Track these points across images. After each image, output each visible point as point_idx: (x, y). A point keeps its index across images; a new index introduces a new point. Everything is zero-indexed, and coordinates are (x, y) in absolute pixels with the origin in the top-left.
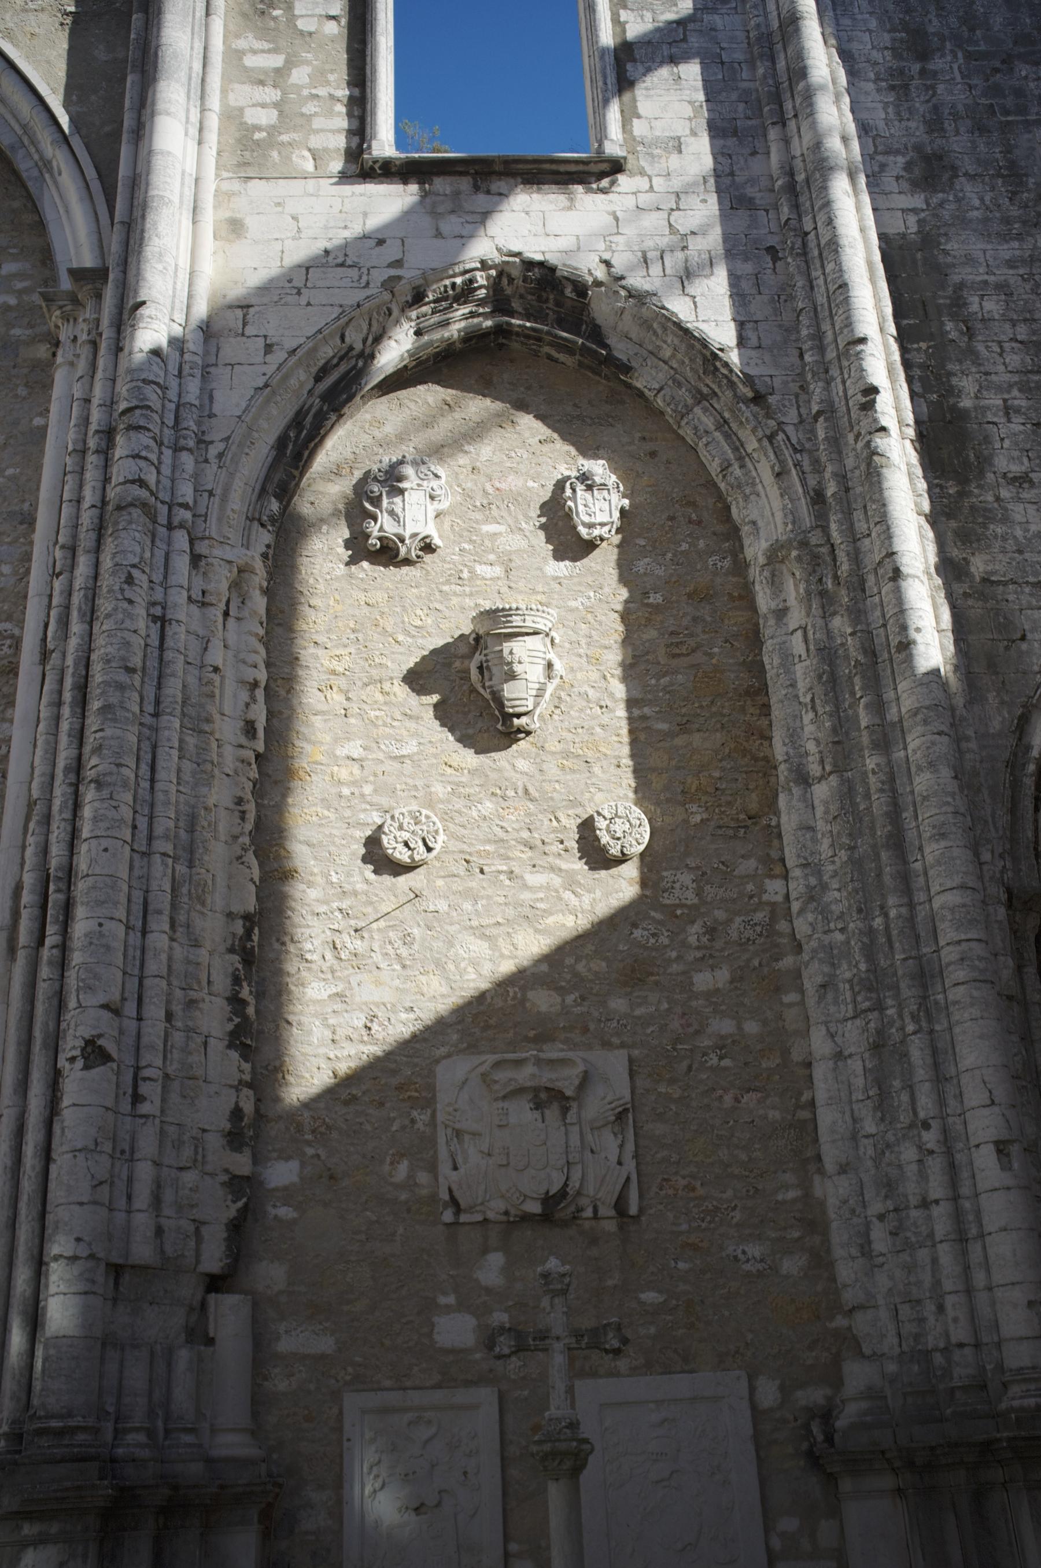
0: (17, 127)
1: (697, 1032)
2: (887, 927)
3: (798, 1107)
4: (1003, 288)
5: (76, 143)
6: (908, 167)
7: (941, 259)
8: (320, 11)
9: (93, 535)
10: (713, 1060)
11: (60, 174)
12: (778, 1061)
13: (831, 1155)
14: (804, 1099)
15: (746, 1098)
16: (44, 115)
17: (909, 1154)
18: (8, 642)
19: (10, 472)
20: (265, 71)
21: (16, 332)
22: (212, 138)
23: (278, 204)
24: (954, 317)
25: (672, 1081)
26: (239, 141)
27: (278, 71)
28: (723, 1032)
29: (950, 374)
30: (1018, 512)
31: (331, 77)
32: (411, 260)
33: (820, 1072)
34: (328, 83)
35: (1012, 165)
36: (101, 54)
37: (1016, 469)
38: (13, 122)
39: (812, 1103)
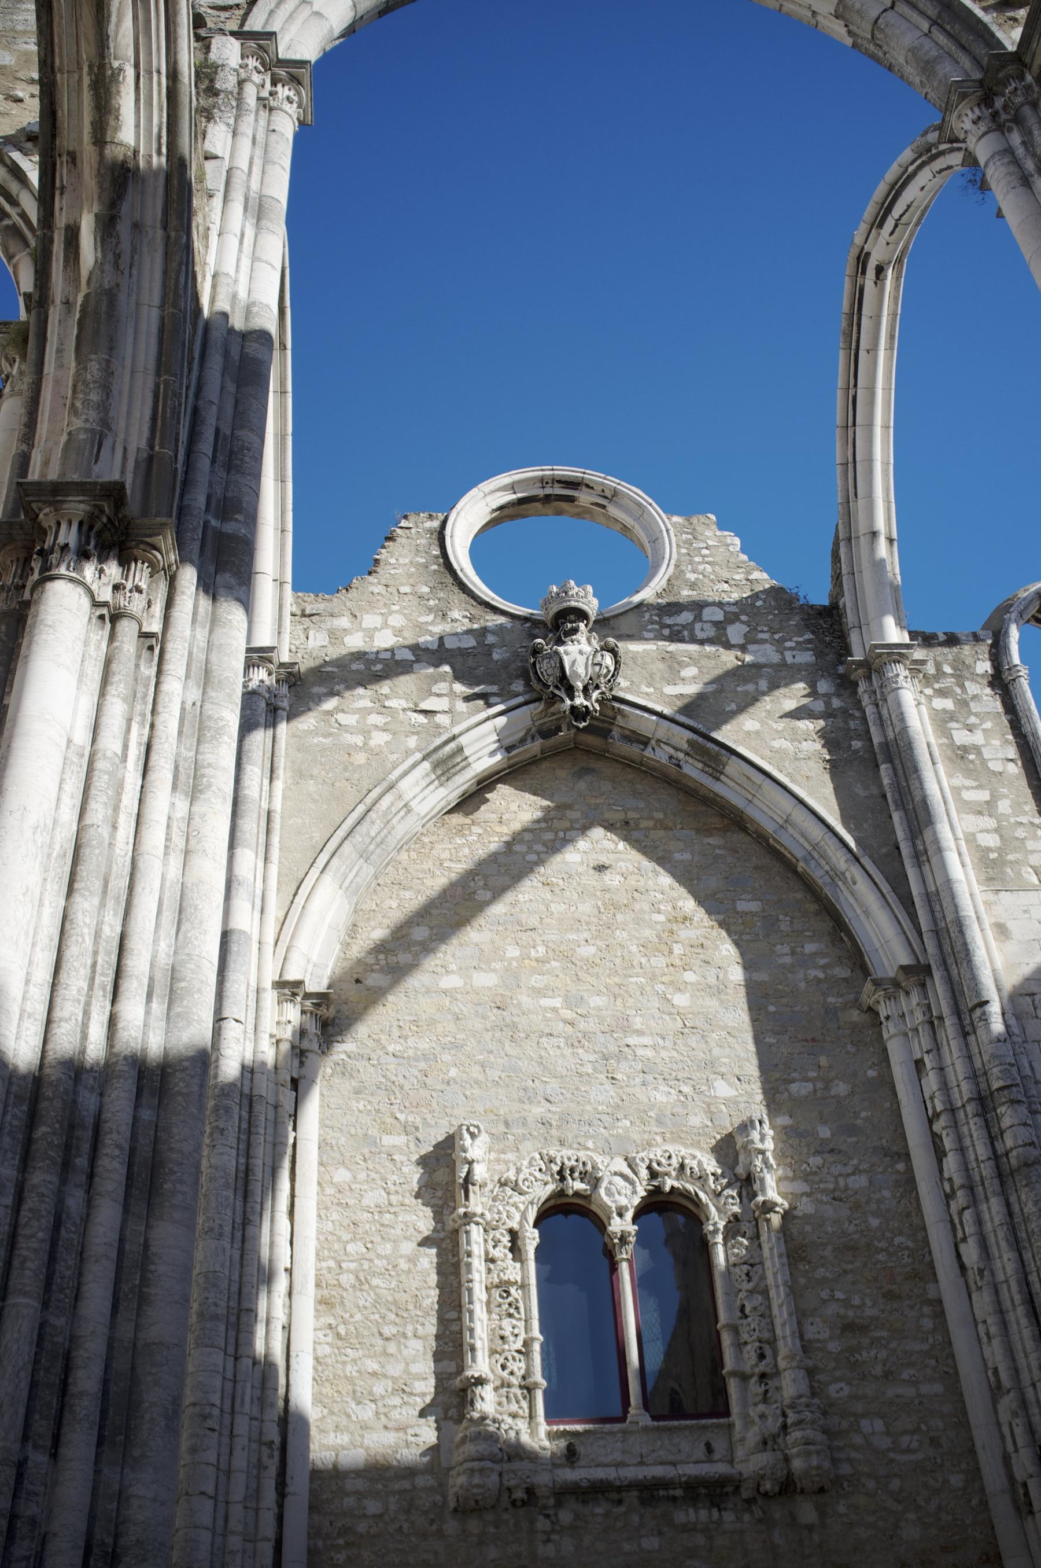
0: (806, 845)
5: (866, 861)
8: (1000, 755)
9: (996, 1181)
11: (855, 883)
16: (835, 839)
18: (906, 1252)
19: (863, 1114)
20: (978, 803)
21: (831, 1000)
22: (968, 860)
23: (1025, 911)
26: (980, 860)
27: (987, 803)
31: (1027, 808)
34: (1025, 813)
36: (860, 791)
38: (802, 841)
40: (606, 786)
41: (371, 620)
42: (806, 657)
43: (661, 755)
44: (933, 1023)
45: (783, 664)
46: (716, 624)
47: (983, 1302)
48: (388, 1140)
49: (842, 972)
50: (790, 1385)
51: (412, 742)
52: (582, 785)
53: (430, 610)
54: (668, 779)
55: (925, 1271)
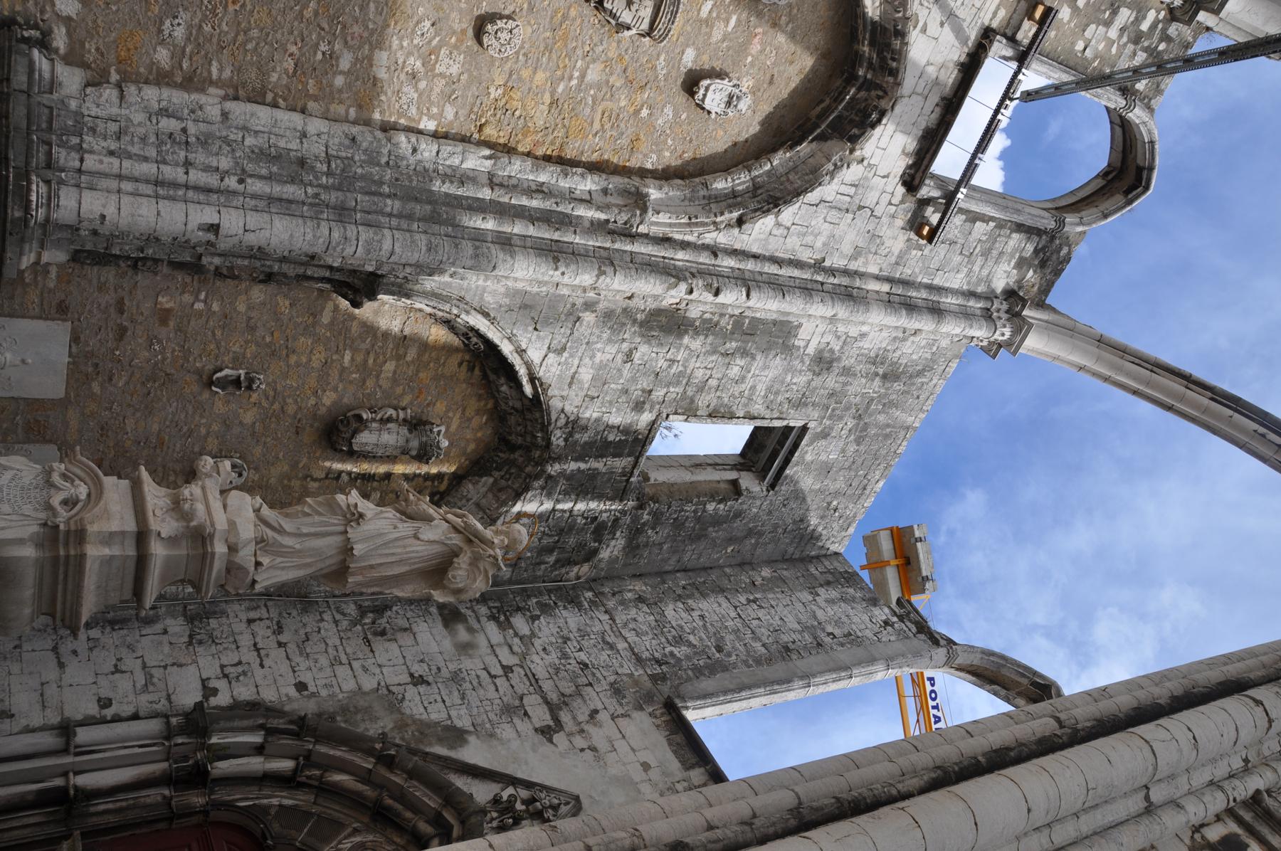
1: (346, 42)
2: (381, 195)
3: (276, 95)
4: (742, 379)
6: (832, 351)
7: (773, 352)
10: (323, 47)
12: (311, 92)
13: (238, 109)
14: (280, 101)
15: (292, 63)
17: (225, 163)
24: (737, 349)
25: (316, 13)
28: (341, 60)
29: (707, 336)
30: (612, 349)
32: (922, 38)
33: (297, 119)
35: (806, 405)
37: (637, 356)
39: (275, 105)
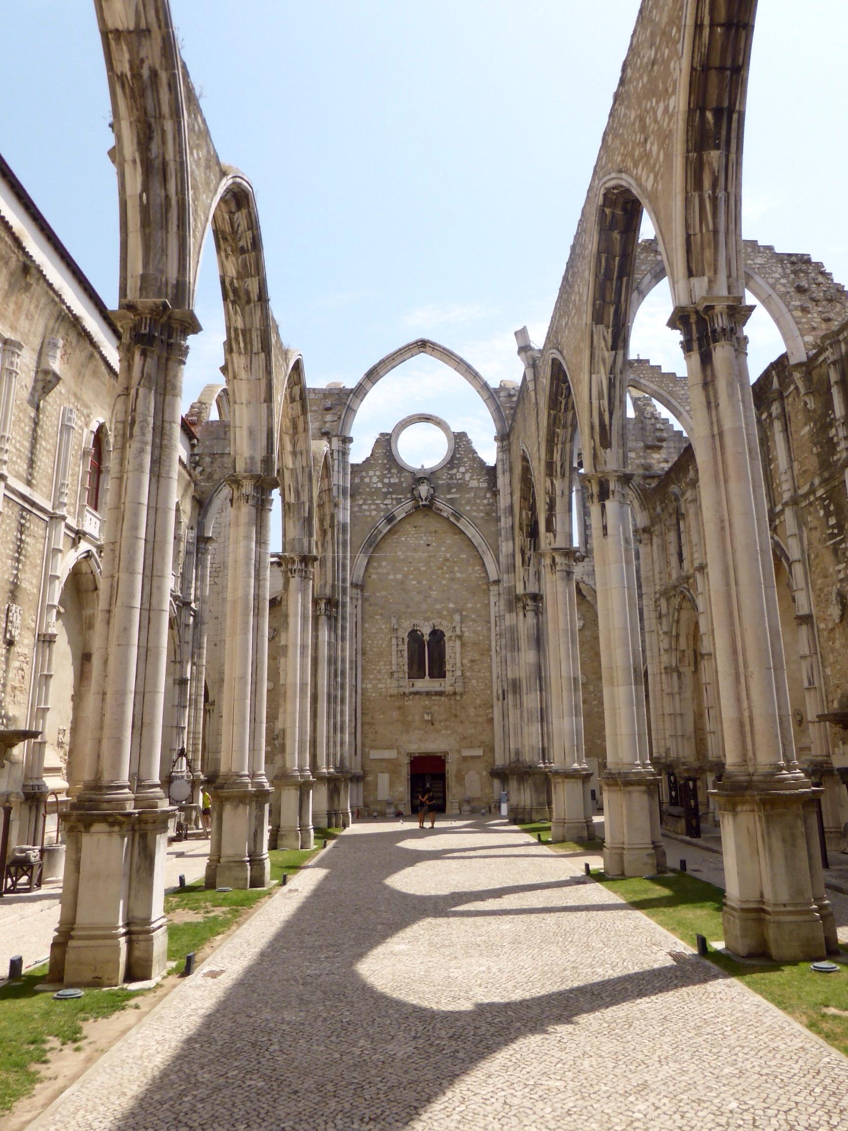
36: (493, 529)
40: (431, 520)
41: (371, 473)
42: (485, 485)
43: (445, 514)
44: (499, 594)
45: (478, 488)
46: (463, 473)
47: (499, 659)
48: (377, 617)
49: (483, 575)
50: (459, 673)
51: (382, 514)
52: (425, 520)
53: (387, 469)
54: (448, 519)
55: (489, 650)
